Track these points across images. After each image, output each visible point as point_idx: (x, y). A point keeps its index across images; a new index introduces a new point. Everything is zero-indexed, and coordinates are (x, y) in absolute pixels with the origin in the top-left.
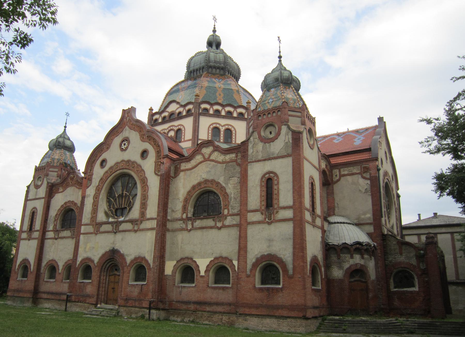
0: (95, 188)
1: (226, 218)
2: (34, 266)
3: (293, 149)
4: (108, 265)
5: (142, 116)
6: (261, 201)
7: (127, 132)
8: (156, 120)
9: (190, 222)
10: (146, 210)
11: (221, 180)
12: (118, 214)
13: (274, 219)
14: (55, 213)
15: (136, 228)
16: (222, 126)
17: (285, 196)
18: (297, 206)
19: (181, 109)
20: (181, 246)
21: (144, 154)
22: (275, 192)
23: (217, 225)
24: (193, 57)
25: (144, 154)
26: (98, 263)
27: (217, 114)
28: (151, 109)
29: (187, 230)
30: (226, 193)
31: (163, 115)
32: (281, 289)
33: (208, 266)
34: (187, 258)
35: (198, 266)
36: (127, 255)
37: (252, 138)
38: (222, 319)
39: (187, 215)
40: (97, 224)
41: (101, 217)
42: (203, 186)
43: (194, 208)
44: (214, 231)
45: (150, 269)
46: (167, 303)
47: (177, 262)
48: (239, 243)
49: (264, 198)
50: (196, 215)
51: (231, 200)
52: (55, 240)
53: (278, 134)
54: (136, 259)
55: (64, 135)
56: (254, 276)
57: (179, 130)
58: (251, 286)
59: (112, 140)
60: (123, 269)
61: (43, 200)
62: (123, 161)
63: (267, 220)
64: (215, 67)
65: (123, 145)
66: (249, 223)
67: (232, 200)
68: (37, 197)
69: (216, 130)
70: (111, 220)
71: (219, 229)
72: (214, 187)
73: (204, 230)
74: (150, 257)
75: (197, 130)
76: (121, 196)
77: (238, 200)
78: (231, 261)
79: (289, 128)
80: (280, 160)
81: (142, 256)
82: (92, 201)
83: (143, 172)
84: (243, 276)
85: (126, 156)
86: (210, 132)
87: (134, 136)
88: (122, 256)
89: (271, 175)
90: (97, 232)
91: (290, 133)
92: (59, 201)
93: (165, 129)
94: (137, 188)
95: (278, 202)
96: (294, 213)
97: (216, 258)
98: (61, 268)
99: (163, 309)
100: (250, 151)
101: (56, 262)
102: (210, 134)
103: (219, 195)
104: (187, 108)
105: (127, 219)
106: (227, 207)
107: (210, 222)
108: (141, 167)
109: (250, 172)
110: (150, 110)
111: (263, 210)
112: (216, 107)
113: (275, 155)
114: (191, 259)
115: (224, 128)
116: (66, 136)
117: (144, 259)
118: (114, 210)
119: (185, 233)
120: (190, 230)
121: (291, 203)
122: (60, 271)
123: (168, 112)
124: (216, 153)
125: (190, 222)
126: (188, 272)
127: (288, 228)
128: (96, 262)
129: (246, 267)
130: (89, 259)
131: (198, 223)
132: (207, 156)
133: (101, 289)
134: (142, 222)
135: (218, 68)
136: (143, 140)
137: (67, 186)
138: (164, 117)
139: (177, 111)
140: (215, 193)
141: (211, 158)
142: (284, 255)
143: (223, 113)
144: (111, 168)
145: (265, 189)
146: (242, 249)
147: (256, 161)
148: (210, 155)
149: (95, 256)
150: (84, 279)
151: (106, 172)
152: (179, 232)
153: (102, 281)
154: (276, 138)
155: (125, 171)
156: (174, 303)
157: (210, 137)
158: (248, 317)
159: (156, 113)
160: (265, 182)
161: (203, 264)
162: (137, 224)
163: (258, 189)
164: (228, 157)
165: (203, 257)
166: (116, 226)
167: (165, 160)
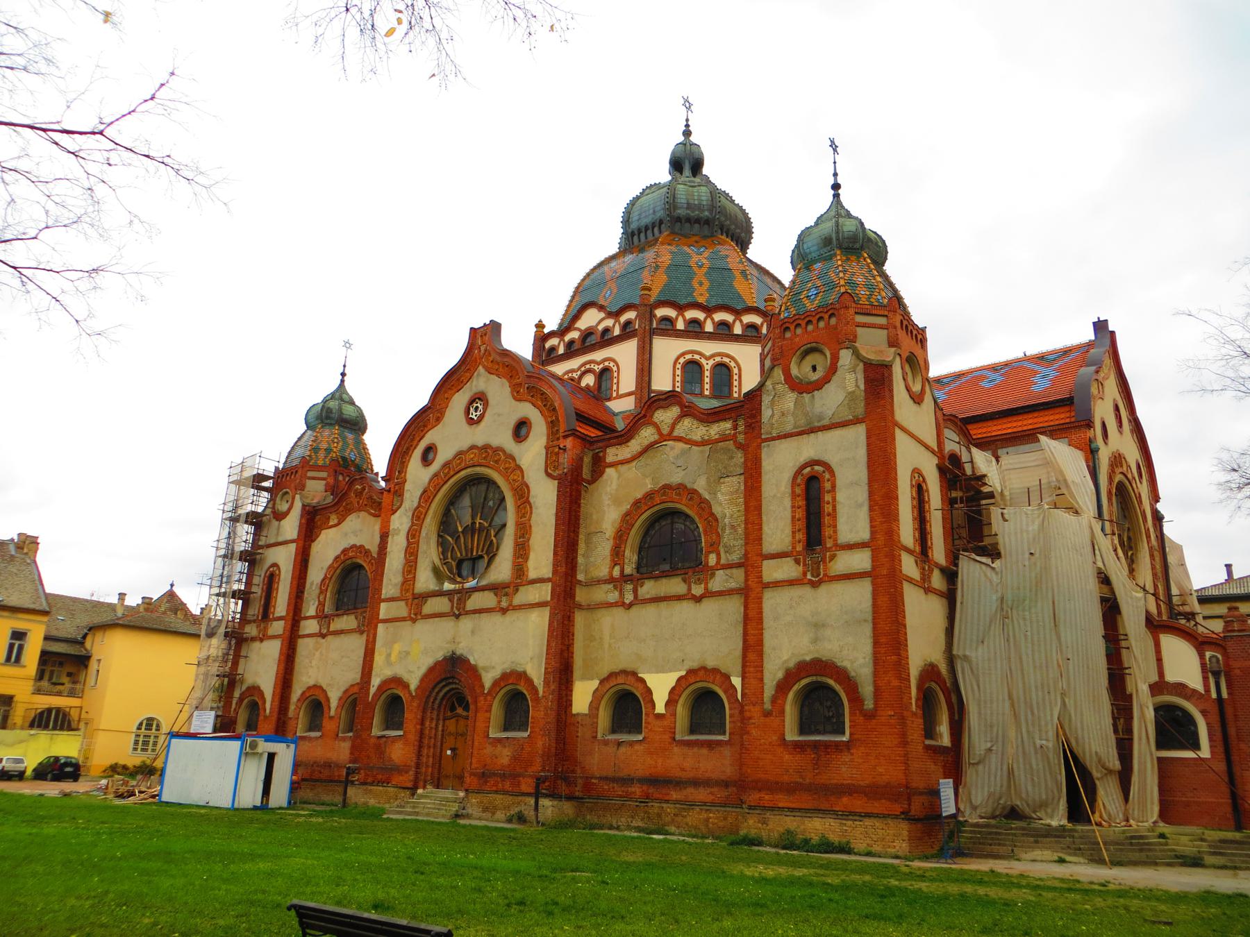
0: (410, 514)
1: (713, 575)
2: (273, 701)
3: (867, 404)
4: (441, 694)
5: (519, 342)
6: (793, 533)
7: (482, 381)
8: (553, 349)
10: (527, 559)
11: (701, 485)
12: (465, 573)
13: (825, 575)
14: (322, 576)
15: (504, 604)
16: (708, 358)
17: (851, 517)
18: (882, 541)
19: (609, 322)
21: (521, 430)
22: (828, 508)
23: (694, 592)
24: (638, 198)
25: (521, 430)
26: (418, 688)
27: (694, 330)
28: (540, 326)
29: (623, 604)
30: (712, 514)
31: (567, 338)
32: (848, 745)
34: (624, 672)
35: (649, 692)
37: (768, 383)
38: (707, 820)
39: (622, 571)
40: (415, 597)
41: (425, 580)
42: (657, 500)
43: (640, 552)
44: (686, 607)
45: (537, 700)
46: (580, 781)
47: (602, 682)
48: (745, 634)
49: (801, 524)
50: (643, 570)
51: (724, 530)
53: (833, 369)
54: (505, 677)
55: (340, 394)
56: (782, 712)
57: (606, 370)
58: (775, 738)
59: (448, 399)
60: (476, 702)
61: (293, 547)
62: (473, 447)
63: (809, 576)
64: (688, 220)
65: (472, 410)
66: (768, 586)
68: (280, 539)
69: (692, 368)
70: (447, 586)
71: (698, 599)
72: (684, 501)
73: (663, 605)
74: (536, 672)
75: (646, 369)
76: (471, 530)
77: (740, 530)
78: (727, 677)
79: (856, 353)
81: (520, 669)
82: (404, 543)
83: (518, 472)
84: (754, 712)
85: (479, 436)
86: (678, 372)
87: (497, 388)
88: (473, 672)
89: (817, 468)
90: (416, 615)
91: (861, 365)
92: (329, 546)
93: (572, 371)
94: (505, 509)
95: (835, 532)
96: (874, 559)
97: (691, 672)
98: (334, 703)
99: (570, 798)
100: (766, 413)
101: (324, 692)
102: (678, 379)
103: (697, 519)
104: (623, 318)
105: (484, 583)
106: (714, 547)
107: (675, 585)
108: (514, 459)
109: (767, 465)
110: (537, 326)
111: (799, 553)
112: (691, 314)
113: (826, 422)
114: (634, 674)
115: (711, 362)
116: (344, 396)
117: (522, 676)
118: (454, 564)
119: (619, 612)
120: (630, 606)
121: (865, 535)
122: (332, 713)
123: (579, 329)
124: (687, 422)
125: (629, 587)
126: (627, 704)
127: (859, 596)
128: (413, 687)
129: (762, 693)
130: (397, 681)
131: (649, 588)
132: (665, 432)
133: (425, 751)
134: (517, 590)
135: (698, 221)
136: (517, 397)
137: (349, 511)
138: (572, 342)
139: (601, 327)
140: (687, 516)
141: (675, 434)
142: (852, 662)
143: (709, 327)
144: (446, 465)
145: (802, 503)
146: (752, 648)
147: (779, 437)
150: (387, 728)
151: (436, 475)
152: (603, 611)
153: (427, 732)
154: (826, 380)
155: (478, 470)
157: (678, 384)
158: (768, 814)
159: (552, 334)
160: (803, 486)
161: (661, 685)
162: (506, 594)
163: (788, 502)
164: (715, 430)
165: (661, 669)
166: (459, 599)
167: (569, 443)
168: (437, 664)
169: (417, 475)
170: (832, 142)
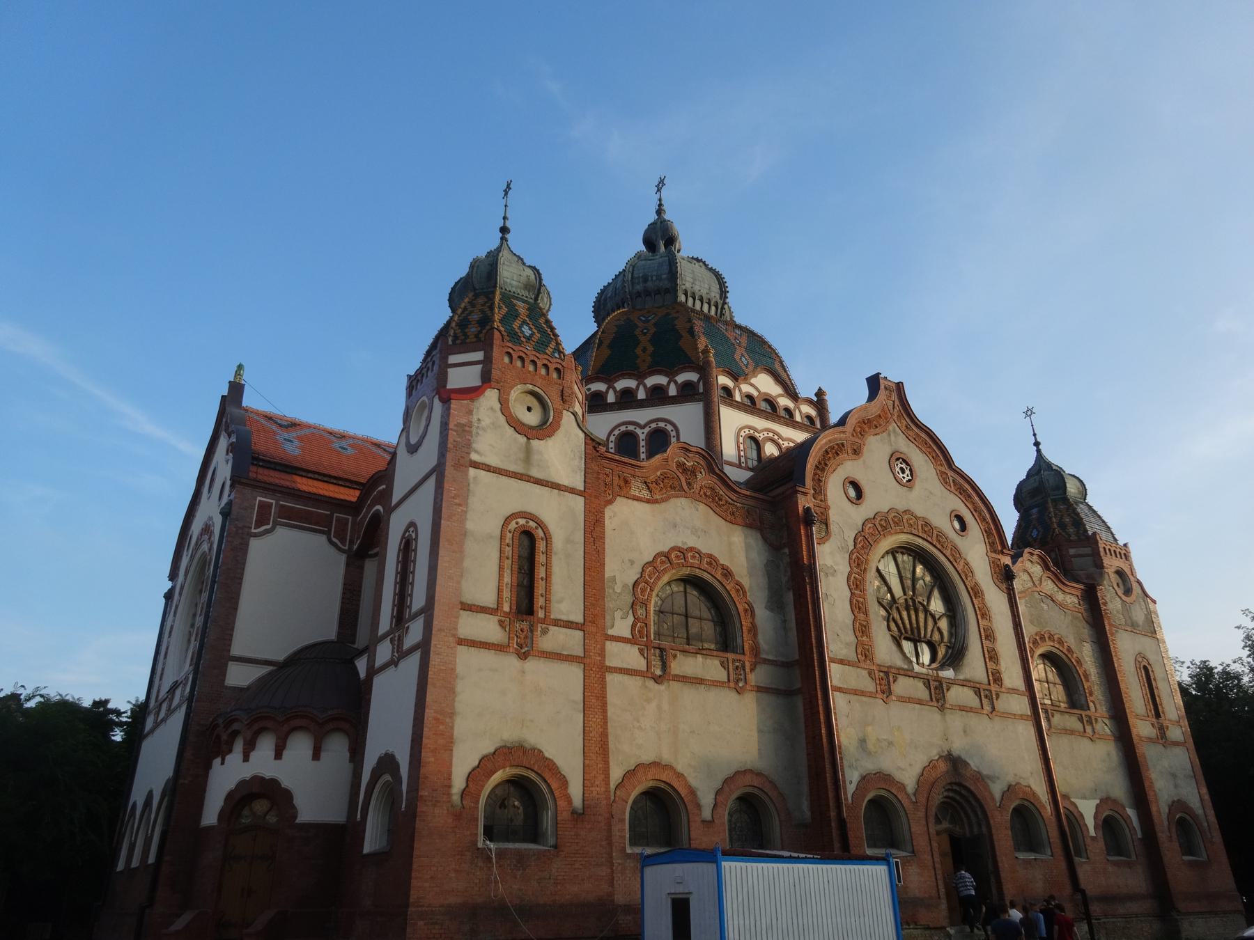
52: (651, 683)
74: (1040, 789)
105: (961, 677)
149: (899, 768)
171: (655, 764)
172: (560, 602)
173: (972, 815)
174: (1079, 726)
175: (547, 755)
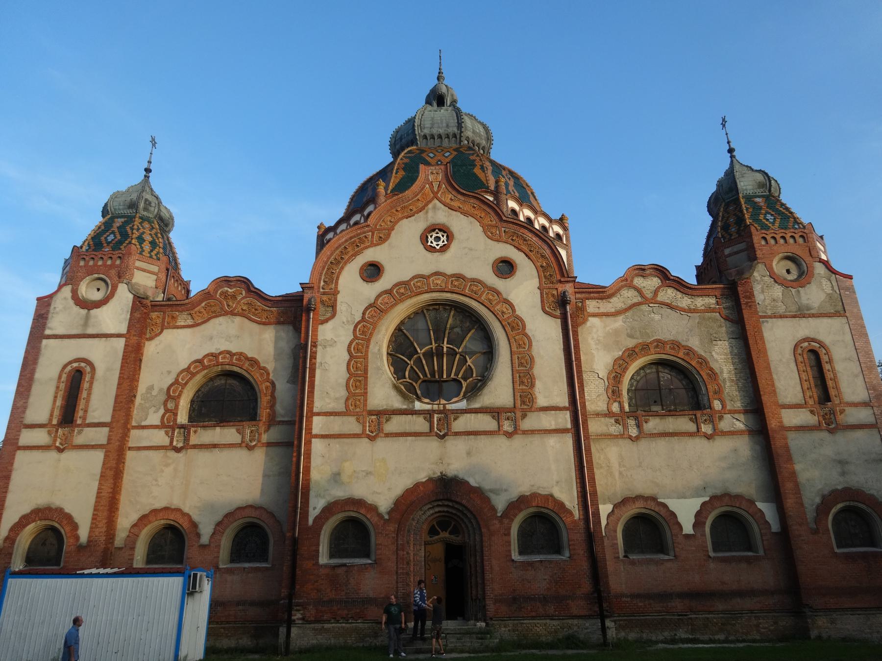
9: (631, 422)
10: (533, 385)
11: (694, 343)
20: (620, 473)
25: (505, 268)
29: (630, 438)
33: (698, 515)
36: (491, 491)
38: (757, 626)
47: (616, 506)
52: (172, 454)
67: (728, 384)
74: (568, 497)
78: (752, 502)
80: (826, 321)
97: (713, 498)
105: (476, 405)
107: (683, 423)
108: (498, 293)
131: (653, 424)
148: (656, 292)
149: (374, 493)
156: (624, 599)
168: (417, 485)
169: (353, 292)
170: (724, 120)
171: (166, 509)
172: (94, 411)
173: (469, 525)
174: (692, 427)
175: (67, 511)
